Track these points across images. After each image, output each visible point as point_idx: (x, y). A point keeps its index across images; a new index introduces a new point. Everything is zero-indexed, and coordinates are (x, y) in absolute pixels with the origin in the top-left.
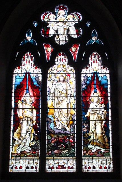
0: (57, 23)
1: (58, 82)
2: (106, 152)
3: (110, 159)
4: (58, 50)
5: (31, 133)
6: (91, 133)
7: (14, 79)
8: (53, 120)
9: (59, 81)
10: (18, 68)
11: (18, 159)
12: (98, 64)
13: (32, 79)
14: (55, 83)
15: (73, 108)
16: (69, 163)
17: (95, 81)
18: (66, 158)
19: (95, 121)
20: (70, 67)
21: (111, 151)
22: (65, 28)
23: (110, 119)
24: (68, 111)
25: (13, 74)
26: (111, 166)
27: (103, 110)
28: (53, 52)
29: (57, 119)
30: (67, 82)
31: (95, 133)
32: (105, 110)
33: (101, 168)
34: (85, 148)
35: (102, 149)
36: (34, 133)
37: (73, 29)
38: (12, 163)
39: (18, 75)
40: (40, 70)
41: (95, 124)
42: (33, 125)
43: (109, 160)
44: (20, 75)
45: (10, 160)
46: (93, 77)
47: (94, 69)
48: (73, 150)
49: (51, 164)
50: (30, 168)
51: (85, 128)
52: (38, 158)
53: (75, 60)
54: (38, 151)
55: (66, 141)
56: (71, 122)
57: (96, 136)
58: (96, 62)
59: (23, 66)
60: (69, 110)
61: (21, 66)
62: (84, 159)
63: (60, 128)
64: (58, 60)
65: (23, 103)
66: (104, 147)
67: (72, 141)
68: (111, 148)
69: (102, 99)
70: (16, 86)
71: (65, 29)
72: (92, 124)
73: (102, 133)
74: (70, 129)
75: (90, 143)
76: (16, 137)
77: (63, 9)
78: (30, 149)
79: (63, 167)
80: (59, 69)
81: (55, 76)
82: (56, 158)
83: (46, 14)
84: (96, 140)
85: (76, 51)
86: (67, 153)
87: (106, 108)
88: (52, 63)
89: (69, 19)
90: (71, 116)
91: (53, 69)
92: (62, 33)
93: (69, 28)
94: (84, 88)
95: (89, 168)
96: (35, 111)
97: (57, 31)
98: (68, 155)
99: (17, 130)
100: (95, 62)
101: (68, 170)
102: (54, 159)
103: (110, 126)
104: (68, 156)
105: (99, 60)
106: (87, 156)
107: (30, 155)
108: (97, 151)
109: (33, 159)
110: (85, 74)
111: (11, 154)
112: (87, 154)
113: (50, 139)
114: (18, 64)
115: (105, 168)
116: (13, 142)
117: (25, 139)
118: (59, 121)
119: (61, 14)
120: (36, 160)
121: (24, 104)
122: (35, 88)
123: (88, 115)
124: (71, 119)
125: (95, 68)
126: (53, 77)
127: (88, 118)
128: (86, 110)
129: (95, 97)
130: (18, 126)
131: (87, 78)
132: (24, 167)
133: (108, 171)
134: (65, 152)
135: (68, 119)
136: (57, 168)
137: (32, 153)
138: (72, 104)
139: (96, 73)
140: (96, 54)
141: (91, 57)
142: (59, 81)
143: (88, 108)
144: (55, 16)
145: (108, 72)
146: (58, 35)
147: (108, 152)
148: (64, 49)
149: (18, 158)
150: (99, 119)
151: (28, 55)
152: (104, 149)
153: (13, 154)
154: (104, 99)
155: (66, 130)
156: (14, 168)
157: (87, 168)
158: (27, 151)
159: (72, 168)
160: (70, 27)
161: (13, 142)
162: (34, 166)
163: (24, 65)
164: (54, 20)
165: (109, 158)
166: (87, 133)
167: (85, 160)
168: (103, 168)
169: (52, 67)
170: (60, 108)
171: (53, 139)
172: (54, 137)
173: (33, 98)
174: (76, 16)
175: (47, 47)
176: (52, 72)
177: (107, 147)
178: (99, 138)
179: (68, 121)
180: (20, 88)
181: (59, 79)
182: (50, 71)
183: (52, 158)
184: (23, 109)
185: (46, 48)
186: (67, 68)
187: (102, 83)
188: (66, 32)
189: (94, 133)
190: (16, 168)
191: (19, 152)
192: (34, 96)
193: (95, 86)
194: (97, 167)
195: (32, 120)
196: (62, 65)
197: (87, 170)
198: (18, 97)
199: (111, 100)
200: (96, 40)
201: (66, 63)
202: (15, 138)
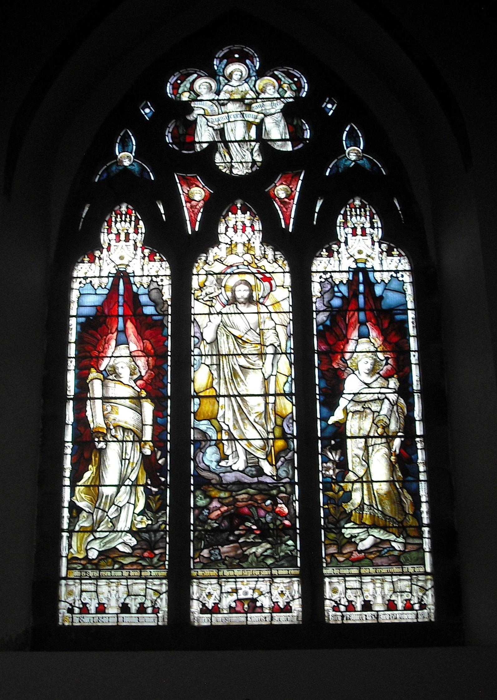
0: (223, 105)
1: (229, 303)
2: (409, 548)
3: (426, 573)
5: (135, 485)
6: (353, 482)
7: (74, 295)
8: (214, 437)
9: (234, 301)
10: (87, 259)
11: (90, 578)
12: (369, 238)
13: (136, 296)
14: (218, 307)
15: (284, 395)
16: (275, 592)
17: (361, 299)
18: (265, 572)
19: (366, 437)
20: (270, 252)
21: (427, 544)
22: (251, 120)
23: (419, 429)
24: (267, 404)
25: (71, 278)
26: (429, 599)
27: (393, 397)
28: (208, 202)
29: (229, 432)
30: (262, 304)
32: (402, 401)
33: (391, 606)
34: (332, 536)
35: (392, 537)
36: (145, 486)
37: (277, 124)
38: (70, 593)
40: (166, 264)
41: (366, 447)
42: (144, 457)
43: (421, 578)
44: (96, 282)
45: (63, 582)
46: (352, 284)
47: (357, 256)
48: (290, 542)
49: (209, 595)
50: (134, 609)
51: (330, 464)
52: (163, 573)
53: (287, 225)
55: (262, 513)
56: (280, 443)
57: (371, 490)
58: (364, 234)
59: (105, 251)
60: (271, 399)
61: (97, 253)
62: (330, 576)
63: (241, 465)
64: (227, 227)
65: (105, 378)
67: (286, 510)
68: (426, 535)
69: (387, 359)
70: (82, 320)
71: (249, 124)
73: (391, 482)
74: (277, 470)
75: (348, 517)
77: (241, 60)
78: (134, 542)
80: (232, 260)
81: (219, 281)
82: (227, 573)
83: (183, 78)
84: (371, 505)
85: (290, 196)
86: (267, 557)
89: (263, 91)
90: (279, 421)
91: (211, 259)
92: (238, 139)
93: (262, 121)
94: (323, 324)
95: (350, 607)
96: (148, 408)
97: (222, 132)
98: (270, 561)
99: (87, 475)
100: (359, 231)
101: (272, 618)
102: (219, 578)
103: (421, 456)
104: (269, 567)
105: (372, 227)
106: (339, 564)
107: (132, 564)
108: (375, 545)
109: (146, 578)
110: (325, 272)
111: (64, 560)
112: (341, 559)
113: (206, 507)
115: (408, 607)
116: (74, 519)
117: (114, 508)
118: (235, 439)
119: (236, 76)
120: (157, 582)
121: (111, 384)
123: (338, 415)
124: (278, 432)
125: (360, 252)
126: (211, 287)
127: (341, 426)
130: (89, 461)
132: (113, 608)
133: (417, 617)
134: (260, 550)
135: (268, 433)
136: (232, 610)
137: (143, 558)
138: (282, 379)
139: (365, 271)
140: (363, 206)
141: (345, 216)
142: (234, 301)
143: (340, 393)
144: (214, 85)
145: (405, 264)
146: (226, 144)
147: (417, 550)
149: (91, 573)
150: (380, 431)
151: (121, 214)
152: (401, 540)
153: (72, 560)
154: (396, 360)
155: (260, 472)
156: (77, 610)
157: (342, 608)
158: (121, 548)
159: (287, 609)
160: (266, 116)
161: (74, 519)
162: (148, 604)
163: (109, 249)
164: (213, 96)
165: (422, 570)
166: (337, 482)
167: (335, 580)
168: (400, 606)
169: (206, 252)
170: (240, 395)
171: (215, 504)
172: (220, 499)
173: (142, 362)
174: (286, 81)
175: (190, 186)
177: (411, 531)
178: (381, 501)
179: (268, 439)
181: (233, 291)
182: (199, 268)
183: (214, 572)
184: (105, 399)
185: (186, 189)
186: (258, 253)
187: (385, 304)
188: (253, 133)
189: (362, 482)
190: (84, 610)
191: (93, 555)
192: (146, 353)
193: (362, 315)
194: (379, 605)
195: (138, 439)
196: (244, 244)
197: (343, 616)
199: (420, 364)
200: (359, 158)
201: (257, 239)
202: (81, 504)
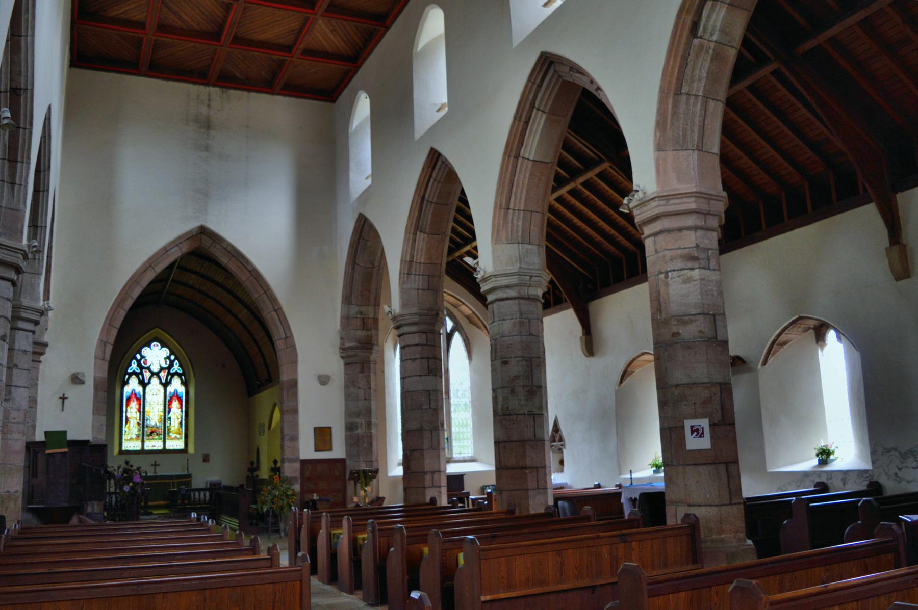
4: (153, 374)
9: (153, 395)
31: (174, 426)
39: (127, 390)
46: (174, 393)
54: (141, 437)
66: (179, 434)
72: (172, 420)
75: (171, 432)
76: (127, 430)
79: (155, 446)
87: (182, 411)
88: (149, 383)
96: (138, 414)
114: (127, 383)
122: (138, 400)
123: (169, 416)
126: (149, 391)
128: (169, 412)
129: (175, 404)
131: (170, 393)
142: (153, 395)
148: (157, 374)
153: (125, 439)
155: (156, 425)
176: (148, 388)
180: (129, 400)
184: (131, 412)
195: (136, 419)
198: (127, 405)
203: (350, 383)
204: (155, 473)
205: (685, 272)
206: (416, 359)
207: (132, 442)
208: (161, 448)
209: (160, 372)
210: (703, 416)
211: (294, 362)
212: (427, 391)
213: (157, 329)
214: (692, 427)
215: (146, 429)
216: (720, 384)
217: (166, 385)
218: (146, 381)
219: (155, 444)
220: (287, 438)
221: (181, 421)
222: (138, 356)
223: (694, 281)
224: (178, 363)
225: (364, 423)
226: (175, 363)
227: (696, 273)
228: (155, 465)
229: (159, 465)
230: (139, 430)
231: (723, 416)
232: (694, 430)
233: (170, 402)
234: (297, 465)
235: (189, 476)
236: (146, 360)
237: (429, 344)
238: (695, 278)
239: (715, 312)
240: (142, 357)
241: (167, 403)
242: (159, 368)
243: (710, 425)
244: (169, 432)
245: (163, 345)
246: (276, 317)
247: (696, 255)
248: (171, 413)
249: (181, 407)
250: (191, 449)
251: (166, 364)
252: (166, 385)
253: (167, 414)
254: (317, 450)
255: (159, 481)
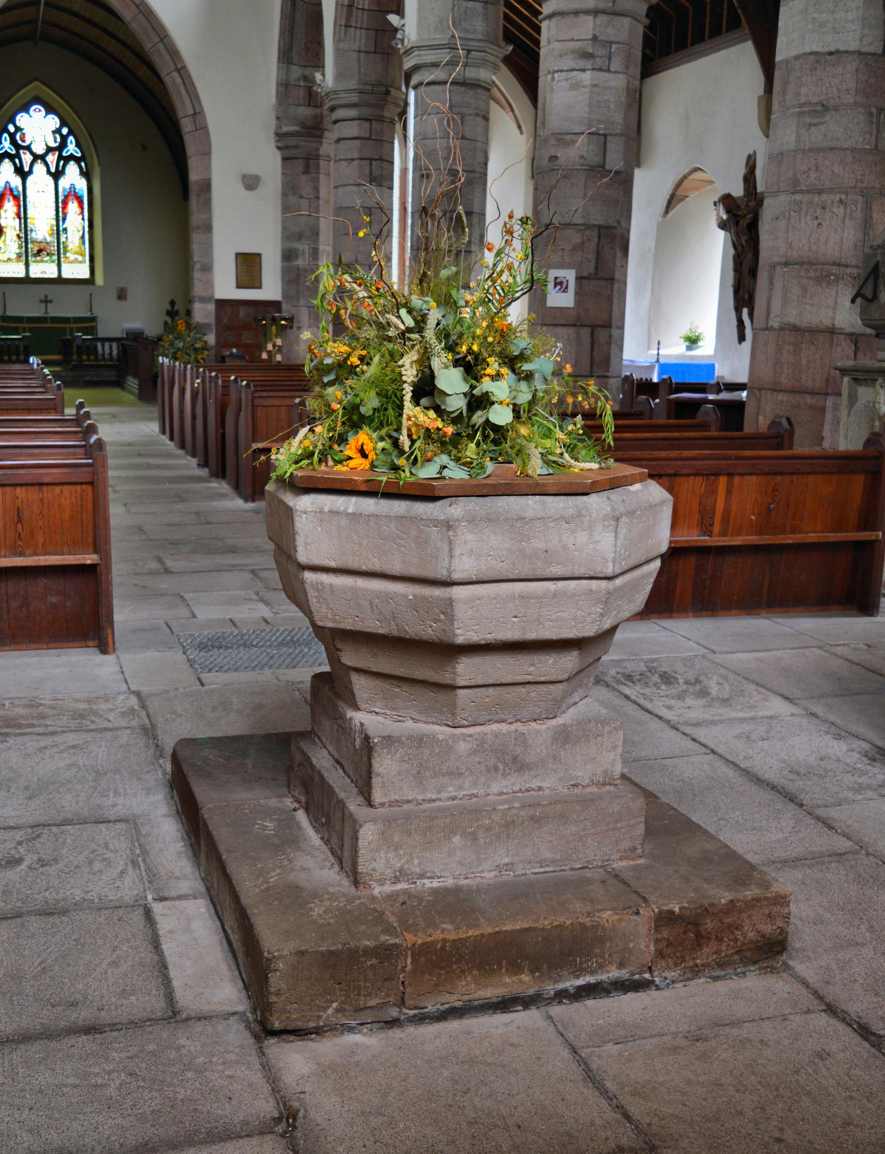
4: (36, 157)
54: (24, 258)
66: (82, 255)
87: (83, 219)
88: (30, 172)
96: (17, 220)
122: (16, 198)
128: (64, 219)
129: (73, 207)
148: (42, 158)
176: (30, 180)
203: (289, 189)
204: (46, 312)
205: (575, 73)
206: (353, 160)
207: (10, 264)
208: (55, 275)
209: (46, 154)
210: (569, 266)
211: (207, 153)
212: (367, 208)
213: (36, 83)
214: (556, 278)
215: (30, 246)
216: (599, 227)
217: (57, 175)
218: (26, 169)
219: (43, 269)
220: (198, 266)
221: (83, 234)
222: (11, 128)
223: (584, 87)
224: (74, 141)
225: (307, 251)
226: (69, 141)
227: (587, 77)
228: (46, 301)
229: (51, 301)
230: (20, 247)
231: (596, 268)
232: (558, 283)
233: (65, 203)
234: (211, 307)
235: (93, 319)
236: (24, 134)
237: (373, 137)
238: (585, 83)
239: (607, 132)
240: (18, 129)
241: (60, 205)
242: (45, 147)
243: (576, 278)
244: (65, 252)
245: (50, 110)
246: (179, 80)
247: (591, 51)
248: (67, 221)
249: (82, 213)
250: (99, 280)
251: (55, 142)
252: (57, 175)
253: (61, 223)
254: (239, 286)
255: (49, 325)
